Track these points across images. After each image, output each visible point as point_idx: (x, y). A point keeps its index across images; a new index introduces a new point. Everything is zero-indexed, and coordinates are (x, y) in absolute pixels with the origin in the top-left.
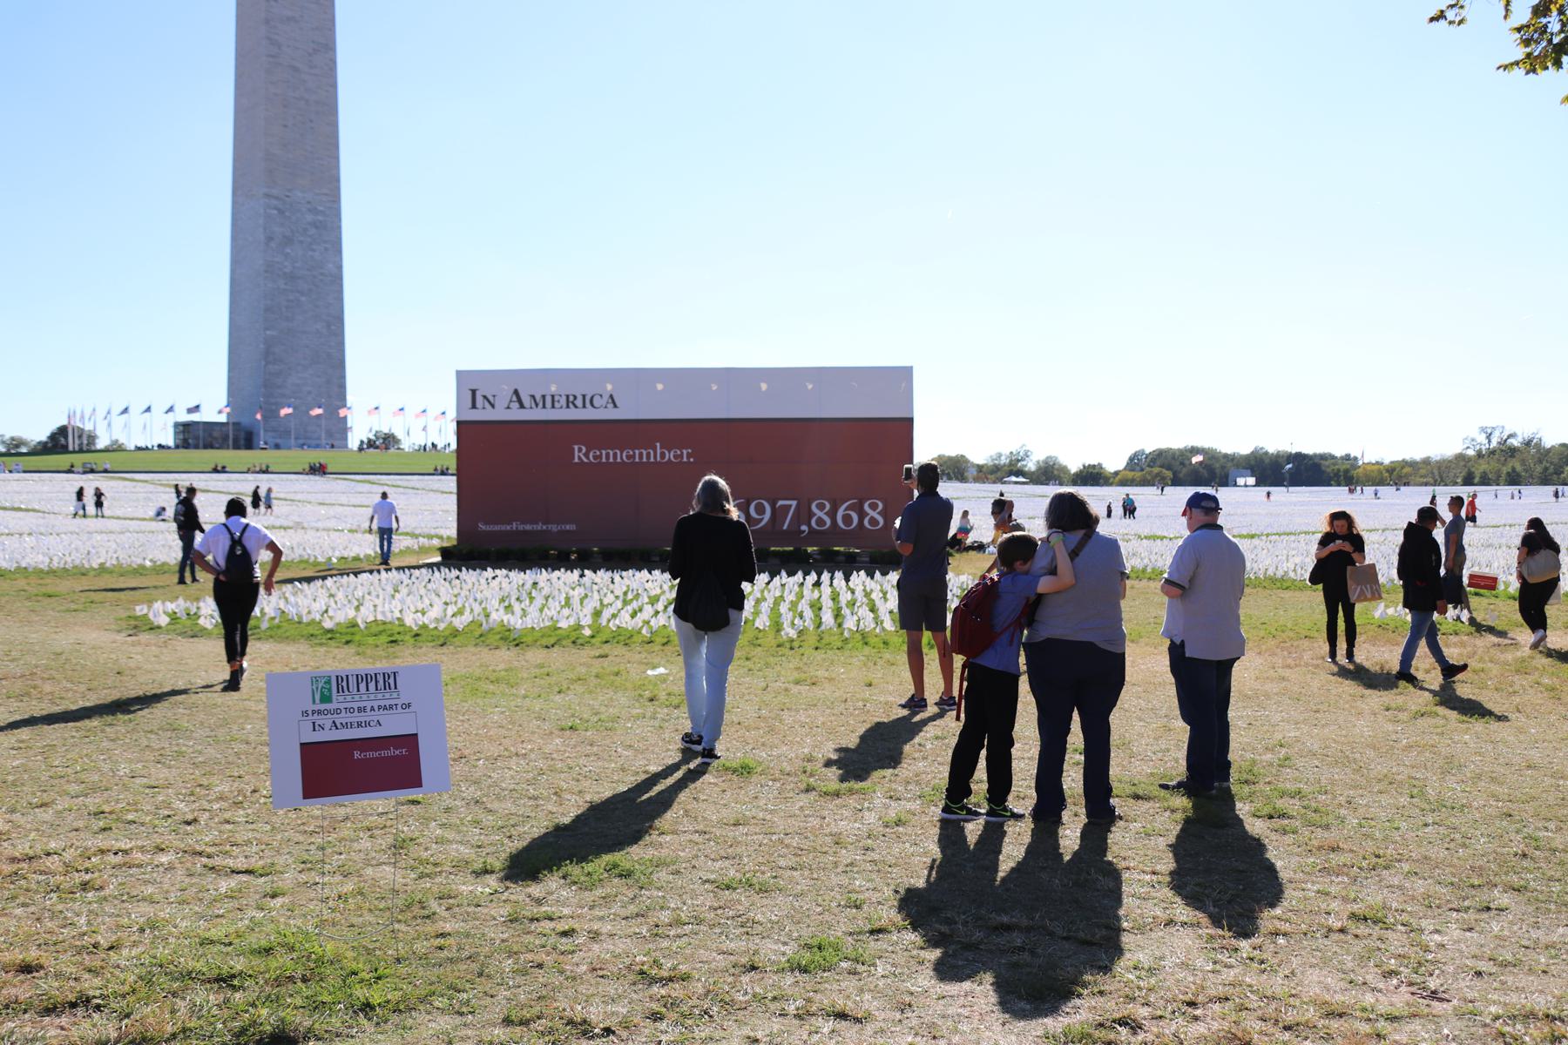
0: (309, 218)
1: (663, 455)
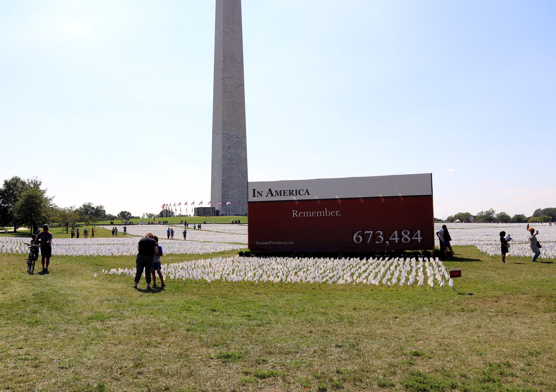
0: (236, 140)
1: (328, 213)
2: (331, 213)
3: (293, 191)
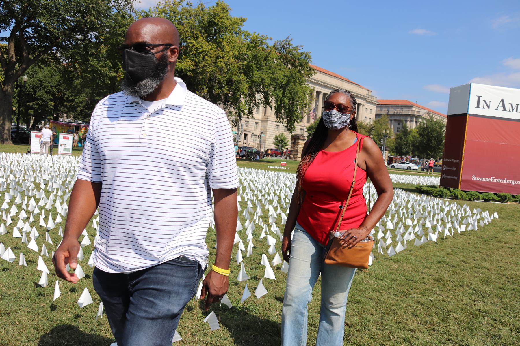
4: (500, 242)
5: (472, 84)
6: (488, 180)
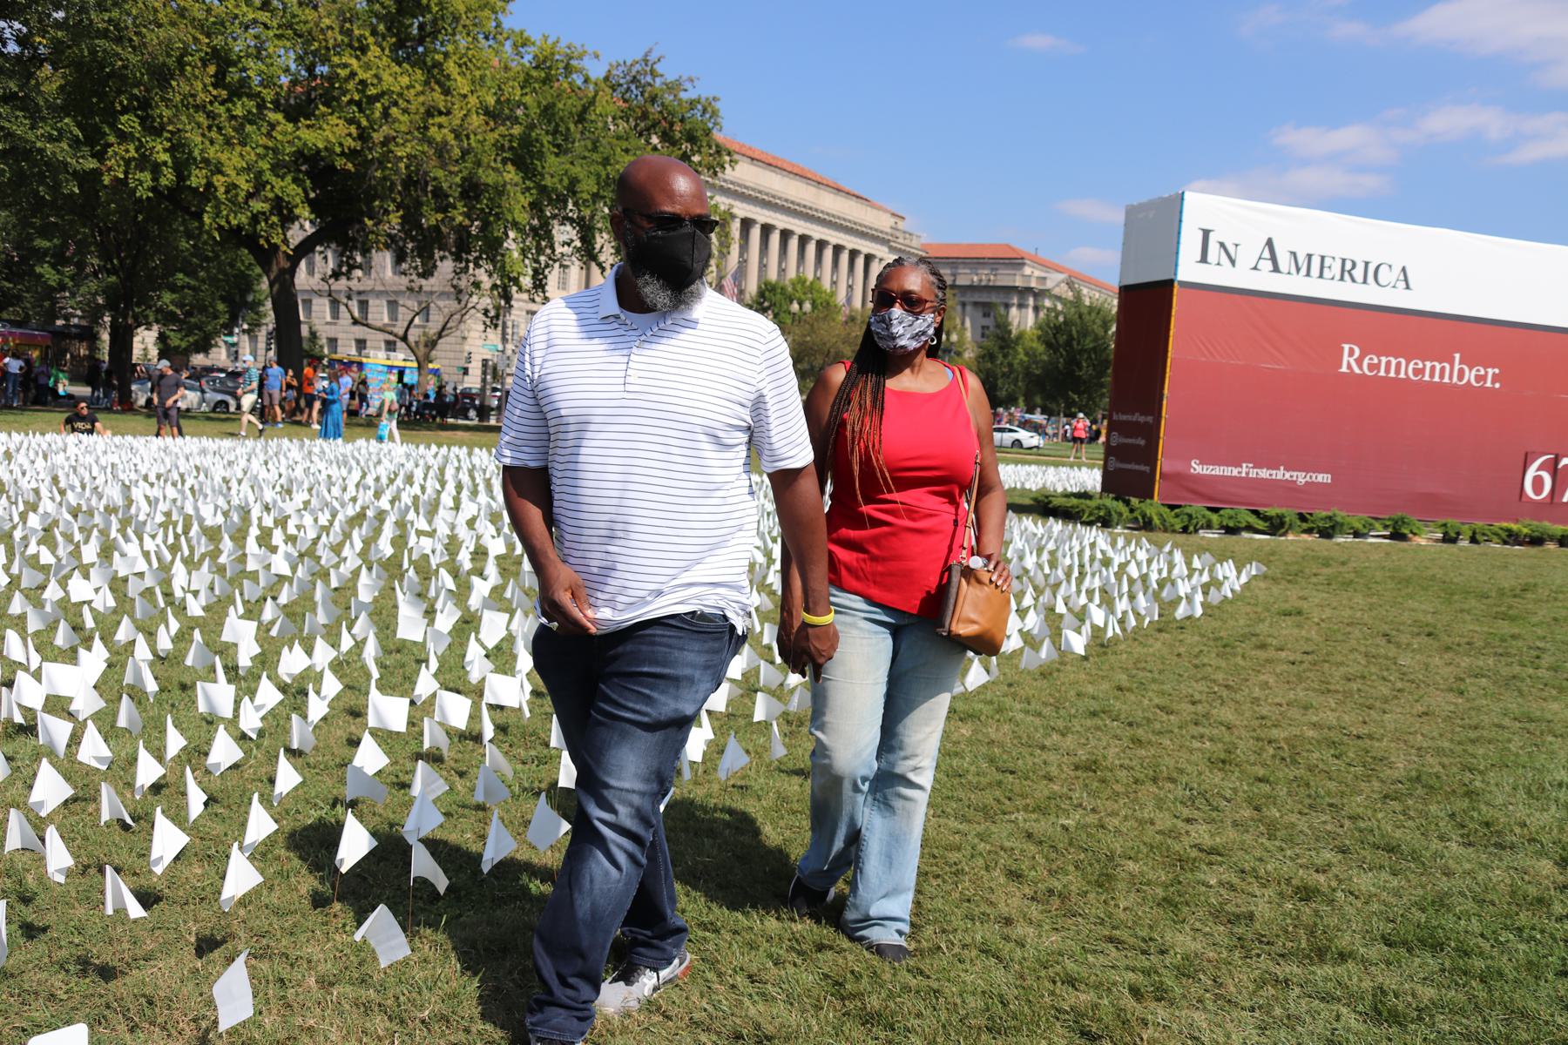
1: (1461, 372)
2: (1470, 376)
3: (1354, 265)
4: (1263, 646)
5: (1187, 195)
6: (1235, 472)
